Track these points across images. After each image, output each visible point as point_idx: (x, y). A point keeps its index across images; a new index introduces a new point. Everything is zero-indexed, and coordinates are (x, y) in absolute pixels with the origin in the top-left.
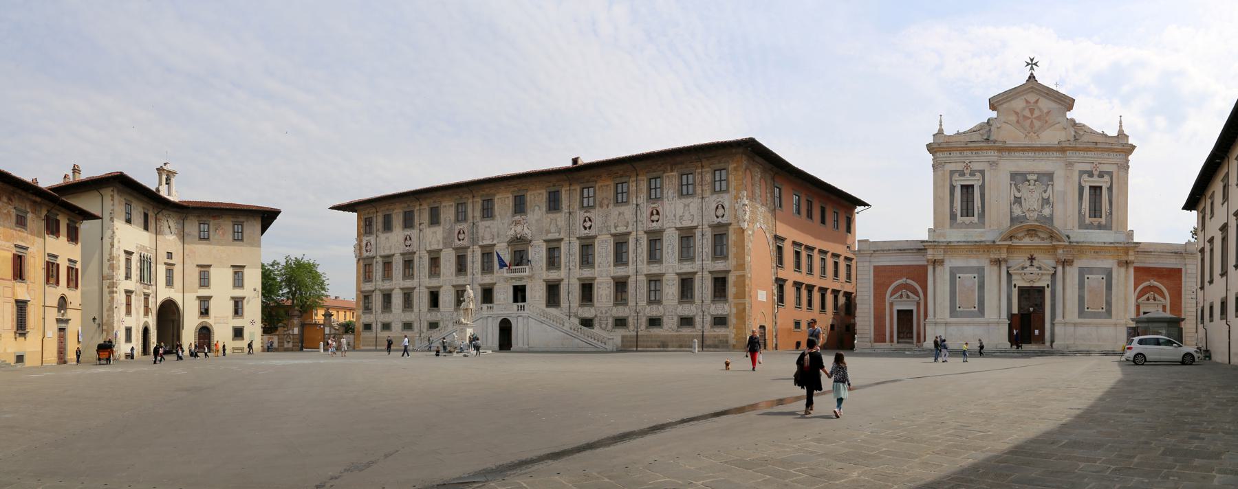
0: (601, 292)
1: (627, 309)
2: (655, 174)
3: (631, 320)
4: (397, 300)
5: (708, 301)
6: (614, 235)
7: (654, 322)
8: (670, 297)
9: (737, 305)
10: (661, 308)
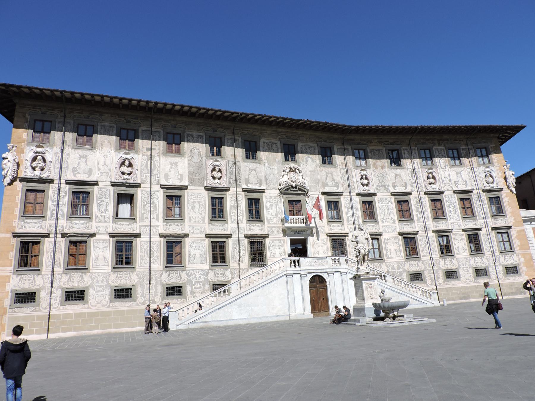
0: (389, 248)
1: (420, 263)
2: (425, 146)
3: (427, 275)
4: (101, 252)
5: (497, 253)
6: (393, 194)
7: (451, 275)
8: (461, 251)
9: (524, 255)
10: (454, 261)
